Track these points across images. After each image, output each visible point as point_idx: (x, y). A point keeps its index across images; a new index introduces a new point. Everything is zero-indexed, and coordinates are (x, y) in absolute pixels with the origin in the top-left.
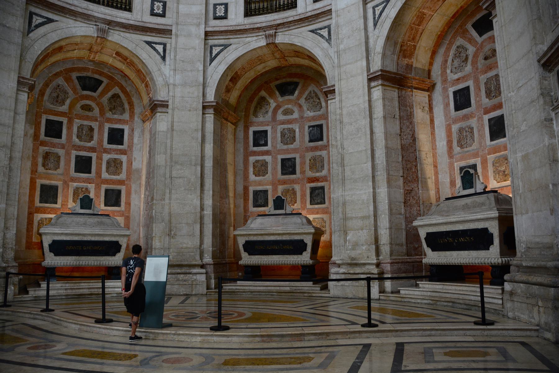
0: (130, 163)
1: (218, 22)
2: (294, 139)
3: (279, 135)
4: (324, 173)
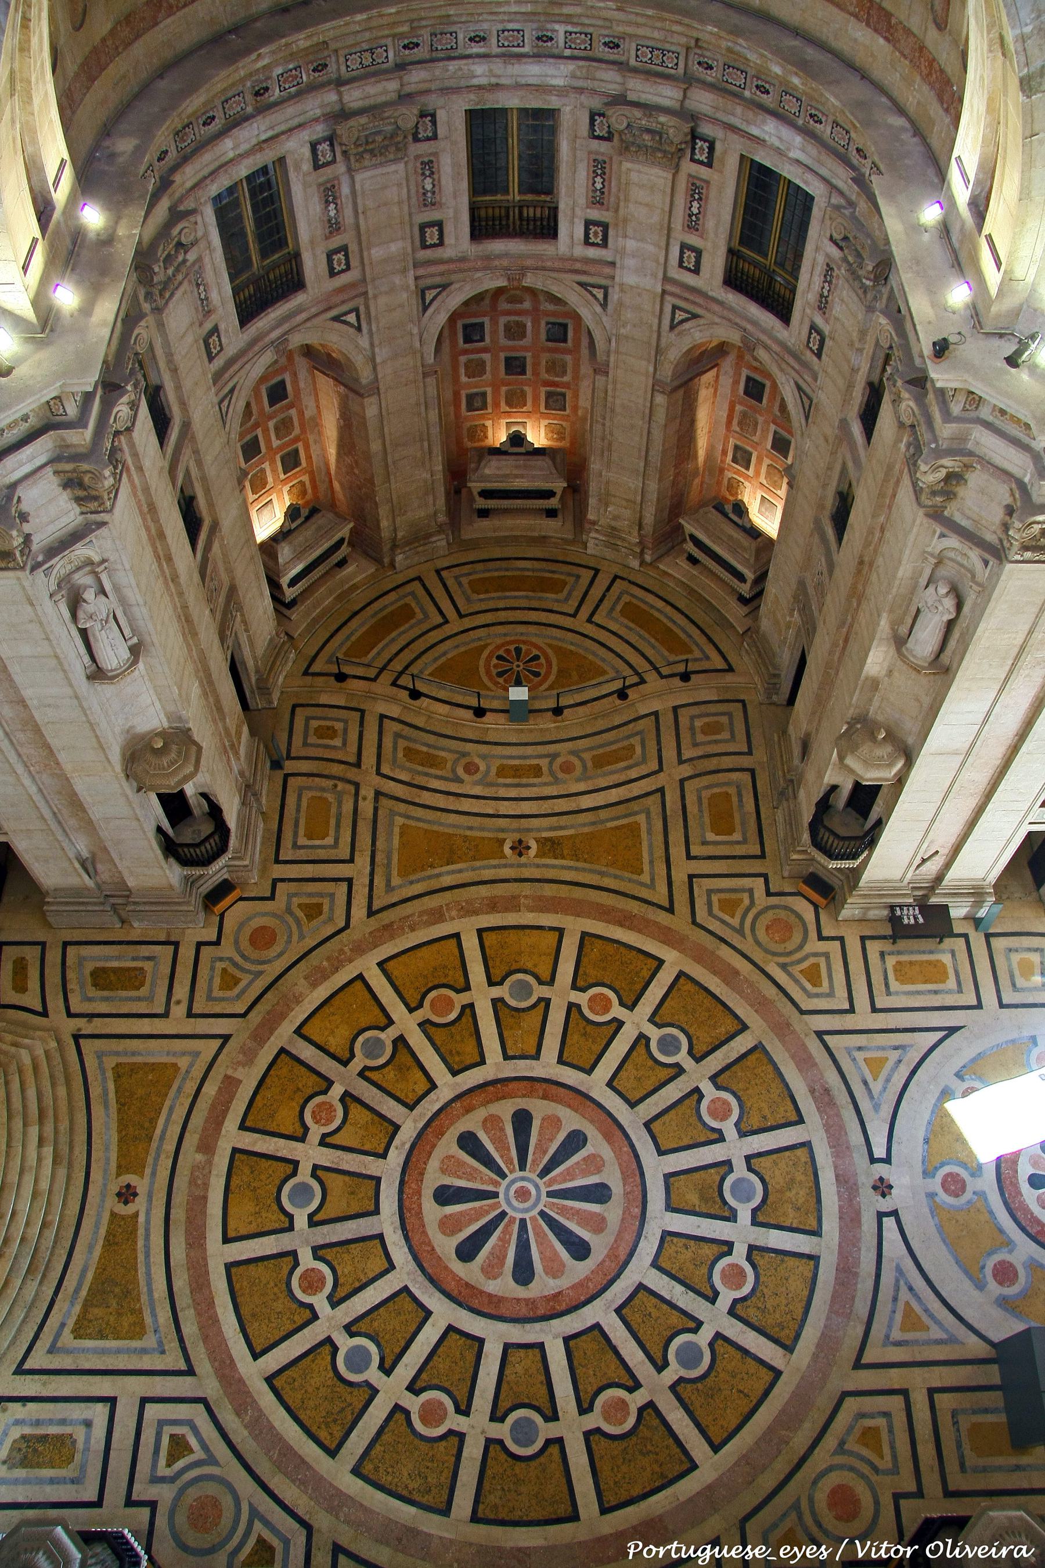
0: (301, 413)
1: (428, 254)
2: (523, 335)
3: (501, 328)
4: (565, 379)
